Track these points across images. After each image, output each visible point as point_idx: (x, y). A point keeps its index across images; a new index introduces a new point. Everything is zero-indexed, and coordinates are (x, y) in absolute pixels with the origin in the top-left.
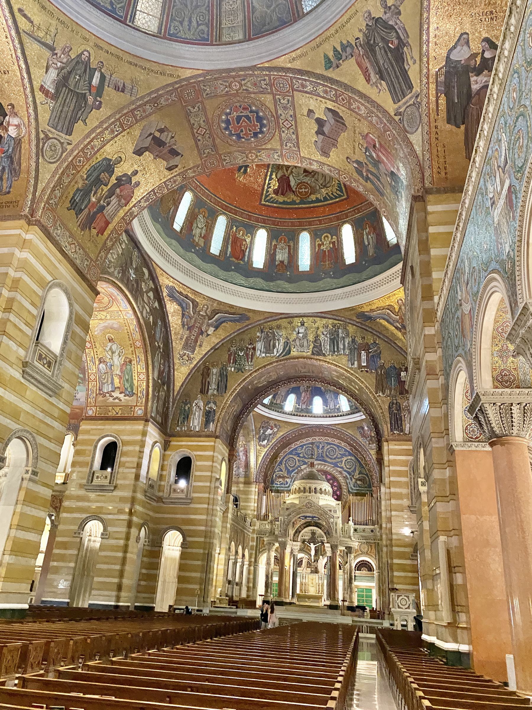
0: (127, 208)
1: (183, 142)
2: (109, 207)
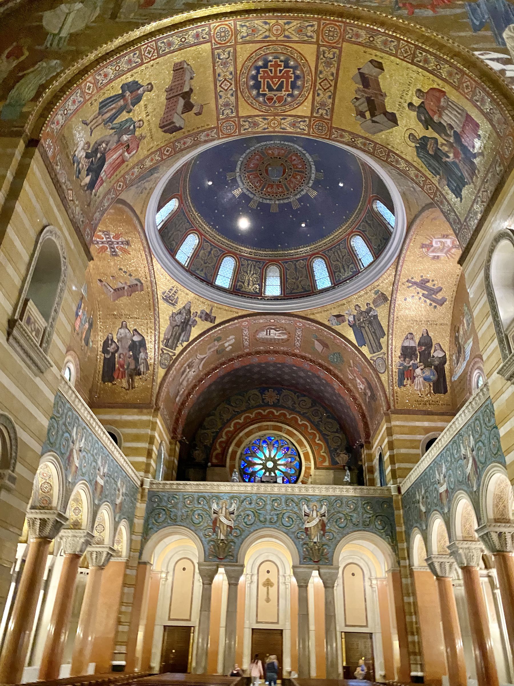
0: (447, 88)
1: (349, 88)
2: (453, 124)
